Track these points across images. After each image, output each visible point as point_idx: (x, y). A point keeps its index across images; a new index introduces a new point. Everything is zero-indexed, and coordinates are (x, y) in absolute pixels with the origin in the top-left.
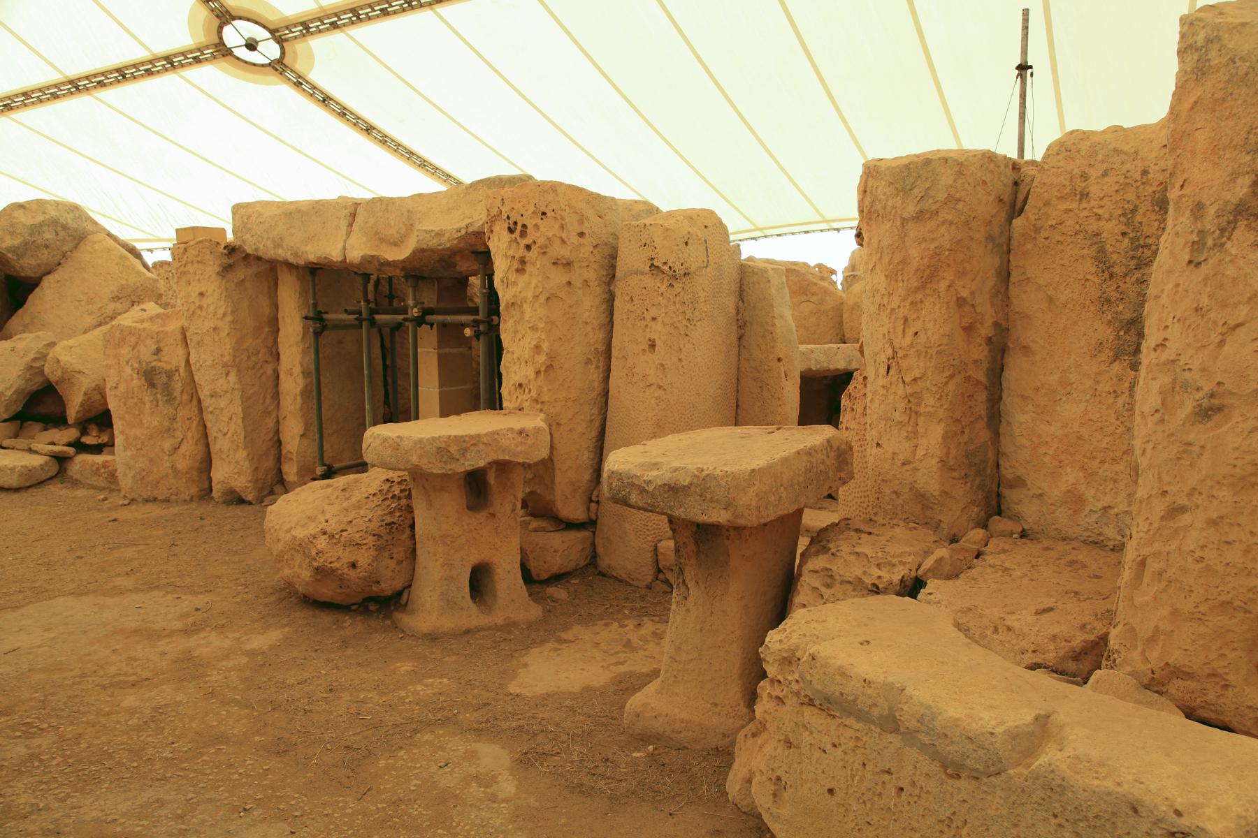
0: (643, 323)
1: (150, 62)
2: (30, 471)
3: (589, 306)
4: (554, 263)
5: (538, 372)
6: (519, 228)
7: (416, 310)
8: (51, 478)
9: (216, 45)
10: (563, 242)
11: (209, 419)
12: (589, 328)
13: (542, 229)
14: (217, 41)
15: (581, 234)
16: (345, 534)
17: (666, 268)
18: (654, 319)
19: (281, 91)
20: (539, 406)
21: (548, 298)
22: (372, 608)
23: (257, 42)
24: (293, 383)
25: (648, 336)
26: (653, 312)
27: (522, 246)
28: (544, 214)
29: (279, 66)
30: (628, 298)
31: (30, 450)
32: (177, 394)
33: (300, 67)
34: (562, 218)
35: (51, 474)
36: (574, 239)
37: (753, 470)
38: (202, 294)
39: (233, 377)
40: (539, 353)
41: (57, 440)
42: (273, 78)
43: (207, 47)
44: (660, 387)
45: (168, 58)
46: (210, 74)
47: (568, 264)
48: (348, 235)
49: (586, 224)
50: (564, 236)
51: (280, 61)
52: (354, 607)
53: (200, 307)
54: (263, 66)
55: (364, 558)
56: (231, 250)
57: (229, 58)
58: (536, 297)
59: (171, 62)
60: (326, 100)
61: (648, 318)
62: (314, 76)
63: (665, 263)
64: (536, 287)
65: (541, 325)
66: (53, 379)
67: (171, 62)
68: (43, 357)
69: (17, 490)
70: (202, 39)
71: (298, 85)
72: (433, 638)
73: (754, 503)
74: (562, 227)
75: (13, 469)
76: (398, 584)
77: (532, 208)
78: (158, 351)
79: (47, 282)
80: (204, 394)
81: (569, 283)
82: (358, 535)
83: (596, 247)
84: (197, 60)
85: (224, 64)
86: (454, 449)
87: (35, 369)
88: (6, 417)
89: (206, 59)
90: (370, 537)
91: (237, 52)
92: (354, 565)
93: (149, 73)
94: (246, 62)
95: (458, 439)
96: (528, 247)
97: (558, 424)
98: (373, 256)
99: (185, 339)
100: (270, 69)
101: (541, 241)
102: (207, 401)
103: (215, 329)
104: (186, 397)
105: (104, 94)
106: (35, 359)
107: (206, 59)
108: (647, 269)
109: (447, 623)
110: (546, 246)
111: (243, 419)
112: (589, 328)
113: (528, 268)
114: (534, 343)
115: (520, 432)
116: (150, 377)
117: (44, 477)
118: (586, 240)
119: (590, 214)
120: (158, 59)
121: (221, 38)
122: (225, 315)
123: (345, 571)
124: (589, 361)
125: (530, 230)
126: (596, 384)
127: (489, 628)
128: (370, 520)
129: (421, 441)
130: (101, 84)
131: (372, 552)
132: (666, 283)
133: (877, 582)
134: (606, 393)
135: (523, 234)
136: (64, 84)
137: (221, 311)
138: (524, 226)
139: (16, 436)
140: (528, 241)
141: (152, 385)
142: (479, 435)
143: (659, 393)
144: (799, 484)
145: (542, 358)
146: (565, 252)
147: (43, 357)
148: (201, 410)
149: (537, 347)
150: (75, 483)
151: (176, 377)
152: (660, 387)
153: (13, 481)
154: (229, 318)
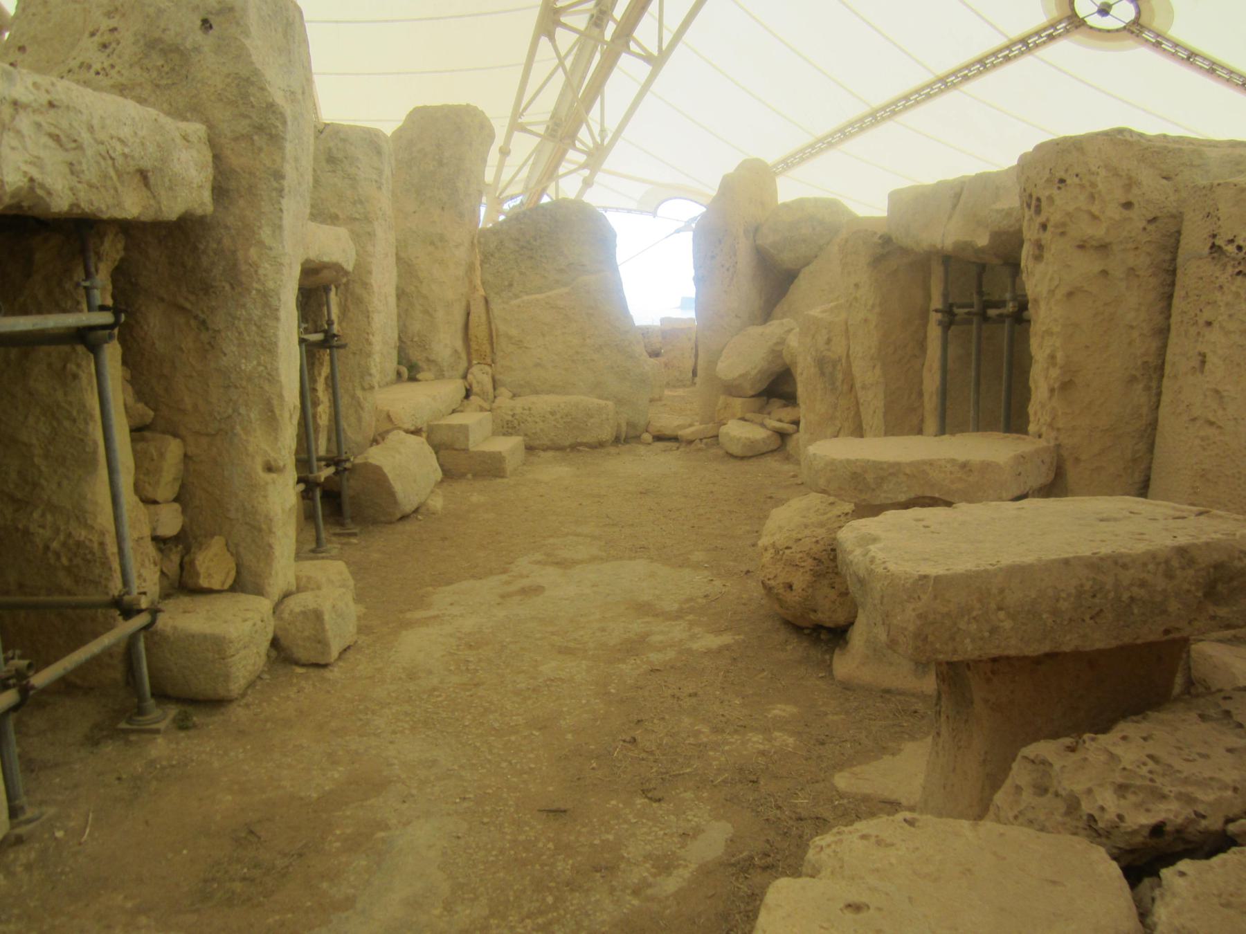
0: (1193, 331)
1: (1008, 47)
2: (752, 443)
3: (1135, 305)
4: (1081, 247)
5: (1052, 390)
6: (1034, 202)
7: (1011, 304)
8: (772, 451)
9: (1069, 18)
10: (1094, 217)
11: (862, 408)
12: (1135, 334)
13: (1058, 202)
14: (1069, 13)
15: (1128, 205)
16: (788, 552)
17: (1231, 249)
18: (1209, 324)
19: (1140, 55)
20: (1054, 434)
21: (1070, 294)
22: (822, 637)
23: (1110, 6)
24: (931, 382)
25: (1201, 348)
26: (1207, 314)
27: (1037, 226)
28: (1062, 181)
29: (1135, 28)
30: (1183, 293)
31: (763, 425)
32: (838, 383)
33: (1157, 24)
34: (1093, 185)
35: (773, 447)
36: (1113, 212)
37: (925, 577)
38: (857, 285)
39: (878, 371)
40: (1054, 365)
41: (778, 417)
42: (1130, 42)
43: (1060, 22)
44: (1211, 424)
45: (1024, 41)
46: (1067, 49)
47: (1103, 248)
48: (950, 218)
49: (1135, 190)
50: (1095, 209)
51: (1136, 22)
52: (806, 631)
53: (856, 299)
54: (1118, 30)
55: (800, 580)
56: (887, 240)
57: (1083, 29)
58: (1052, 292)
59: (1026, 44)
60: (1190, 57)
61: (1201, 322)
62: (1178, 31)
63: (1231, 241)
64: (1051, 279)
65: (1056, 329)
66: (788, 362)
67: (1026, 44)
68: (782, 342)
69: (742, 458)
70: (1055, 14)
71: (1157, 45)
72: (847, 687)
73: (911, 628)
74: (1092, 197)
75: (739, 439)
76: (840, 618)
77: (1046, 175)
78: (829, 341)
79: (801, 276)
80: (858, 385)
81: (1104, 273)
82: (799, 555)
83: (1154, 219)
84: (1051, 38)
85: (1077, 36)
86: (870, 477)
87: (776, 353)
88: (752, 393)
89: (1060, 35)
90: (810, 561)
91: (1091, 21)
92: (790, 587)
93: (1007, 59)
94: (1100, 30)
95: (877, 466)
96: (1044, 227)
97: (1077, 460)
98: (966, 243)
99: (847, 330)
100: (1125, 33)
101: (1056, 217)
102: (860, 394)
103: (866, 320)
104: (845, 387)
105: (969, 87)
106: (777, 344)
107: (1060, 35)
108: (1207, 250)
109: (867, 675)
110: (1064, 224)
111: (885, 414)
112: (1135, 334)
113: (1047, 255)
114: (1048, 351)
115: (964, 466)
116: (821, 362)
117: (765, 449)
118: (1133, 214)
119: (1147, 178)
120: (1014, 44)
121: (1073, 9)
122: (873, 306)
123: (781, 591)
124: (1133, 379)
125: (1044, 204)
126: (1145, 410)
127: (913, 695)
128: (817, 542)
129: (832, 462)
130: (966, 78)
131: (808, 577)
132: (1230, 270)
133: (1097, 814)
134: (1153, 425)
135: (1038, 210)
136: (934, 83)
137: (870, 302)
138: (1038, 200)
139: (760, 410)
140: (1042, 219)
141: (822, 374)
142: (898, 464)
143: (1210, 431)
144: (1055, 612)
145: (1055, 373)
146: (1098, 232)
147: (782, 342)
148: (857, 403)
149: (1052, 357)
150: (788, 458)
151: (839, 367)
152: (1211, 424)
153: (736, 450)
154: (877, 310)
